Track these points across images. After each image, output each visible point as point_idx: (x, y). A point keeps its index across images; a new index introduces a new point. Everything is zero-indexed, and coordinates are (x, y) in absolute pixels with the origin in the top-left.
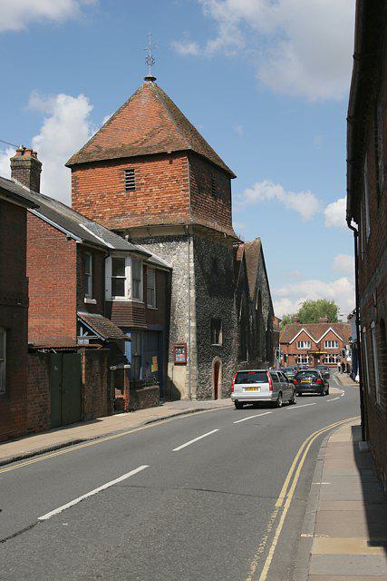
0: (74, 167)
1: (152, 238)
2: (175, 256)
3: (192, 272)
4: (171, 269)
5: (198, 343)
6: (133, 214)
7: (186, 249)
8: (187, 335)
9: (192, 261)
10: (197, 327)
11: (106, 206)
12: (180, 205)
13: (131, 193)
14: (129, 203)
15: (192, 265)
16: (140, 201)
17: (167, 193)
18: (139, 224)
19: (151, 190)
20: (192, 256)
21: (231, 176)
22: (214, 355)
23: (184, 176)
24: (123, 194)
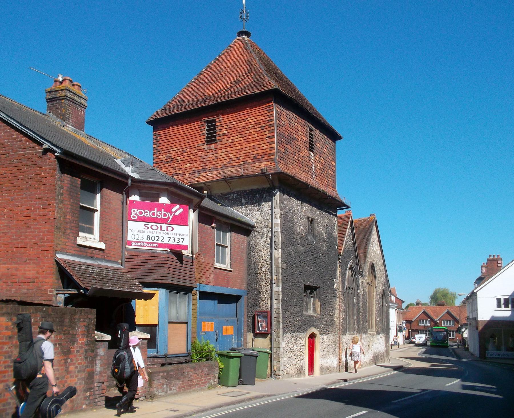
4: (253, 227)
5: (284, 310)
6: (214, 169)
14: (209, 157)
16: (221, 154)
17: (250, 142)
18: (219, 177)
22: (310, 326)
23: (269, 121)
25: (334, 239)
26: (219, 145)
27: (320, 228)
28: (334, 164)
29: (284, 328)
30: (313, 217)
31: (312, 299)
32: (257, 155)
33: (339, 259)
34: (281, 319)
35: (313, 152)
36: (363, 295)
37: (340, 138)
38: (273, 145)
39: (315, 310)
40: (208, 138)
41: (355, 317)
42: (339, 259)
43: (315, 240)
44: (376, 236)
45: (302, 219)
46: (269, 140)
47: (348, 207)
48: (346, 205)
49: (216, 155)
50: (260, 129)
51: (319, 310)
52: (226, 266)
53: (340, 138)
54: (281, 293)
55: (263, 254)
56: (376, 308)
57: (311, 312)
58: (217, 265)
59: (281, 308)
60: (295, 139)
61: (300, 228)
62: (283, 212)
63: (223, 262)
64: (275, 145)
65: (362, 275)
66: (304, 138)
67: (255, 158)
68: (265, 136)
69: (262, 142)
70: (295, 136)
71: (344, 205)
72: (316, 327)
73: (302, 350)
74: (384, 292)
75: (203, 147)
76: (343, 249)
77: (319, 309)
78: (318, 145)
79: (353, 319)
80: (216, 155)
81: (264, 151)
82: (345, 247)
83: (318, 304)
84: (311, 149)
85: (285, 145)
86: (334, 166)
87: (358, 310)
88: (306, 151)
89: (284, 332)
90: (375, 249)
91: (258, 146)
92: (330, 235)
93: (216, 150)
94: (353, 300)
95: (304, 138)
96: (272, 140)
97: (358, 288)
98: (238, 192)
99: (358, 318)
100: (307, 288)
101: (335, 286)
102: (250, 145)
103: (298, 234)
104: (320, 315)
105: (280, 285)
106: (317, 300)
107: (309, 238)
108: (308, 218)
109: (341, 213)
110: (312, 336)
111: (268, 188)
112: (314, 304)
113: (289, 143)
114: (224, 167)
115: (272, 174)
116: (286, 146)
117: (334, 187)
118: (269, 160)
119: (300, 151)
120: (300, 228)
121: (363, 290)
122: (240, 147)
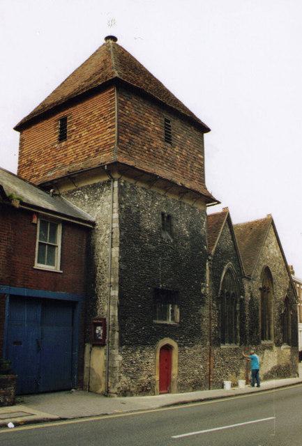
0: (21, 127)
1: (79, 190)
2: (99, 208)
3: (116, 225)
4: (94, 224)
6: (64, 166)
7: (110, 197)
8: (106, 308)
9: (115, 210)
10: (121, 295)
11: (41, 163)
12: (105, 145)
13: (63, 144)
15: (116, 216)
16: (70, 150)
17: (95, 135)
19: (81, 136)
20: (116, 205)
21: (204, 129)
24: (56, 146)
25: (202, 238)
26: (69, 141)
27: (181, 226)
28: (202, 157)
29: (120, 337)
30: (170, 212)
31: (170, 305)
32: (99, 147)
33: (209, 260)
34: (117, 328)
35: (170, 143)
36: (252, 301)
37: (208, 130)
38: (114, 135)
39: (173, 319)
40: (60, 136)
41: (238, 327)
42: (209, 260)
43: (173, 238)
44: (274, 238)
45: (153, 214)
46: (109, 130)
47: (219, 203)
48: (216, 201)
49: (65, 152)
50: (102, 120)
51: (178, 318)
52: (56, 268)
53: (208, 130)
54: (117, 298)
55: (101, 254)
56: (274, 316)
57: (169, 322)
58: (38, 266)
59: (117, 314)
60: (145, 129)
61: (150, 223)
62: (123, 206)
63: (51, 262)
64: (115, 135)
65: (249, 279)
66: (157, 128)
67: (97, 151)
68: (107, 127)
69: (104, 134)
70: (144, 126)
71: (215, 200)
72: (175, 339)
73: (150, 364)
74: (287, 300)
75: (56, 146)
76: (214, 250)
77: (178, 318)
78: (179, 137)
79: (236, 328)
80: (65, 152)
81: (105, 142)
82: (217, 248)
83: (177, 311)
84: (168, 139)
85: (130, 135)
86: (203, 160)
87: (243, 319)
88: (160, 142)
89: (121, 343)
90: (272, 252)
91: (101, 138)
92: (195, 233)
93: (67, 146)
94: (235, 307)
95: (157, 128)
96: (113, 130)
97: (243, 293)
98: (82, 188)
99: (242, 327)
100: (157, 292)
101: (203, 290)
102: (94, 138)
103: (147, 231)
104: (179, 323)
105: (117, 288)
106: (176, 306)
107: (164, 236)
108: (163, 214)
109: (212, 210)
110: (167, 348)
111: (109, 181)
112: (173, 311)
113: (136, 132)
114: (71, 163)
115: (108, 165)
116: (133, 136)
117: (203, 181)
118: (109, 151)
119: (151, 141)
120: (150, 223)
121: (251, 296)
122: (85, 142)
